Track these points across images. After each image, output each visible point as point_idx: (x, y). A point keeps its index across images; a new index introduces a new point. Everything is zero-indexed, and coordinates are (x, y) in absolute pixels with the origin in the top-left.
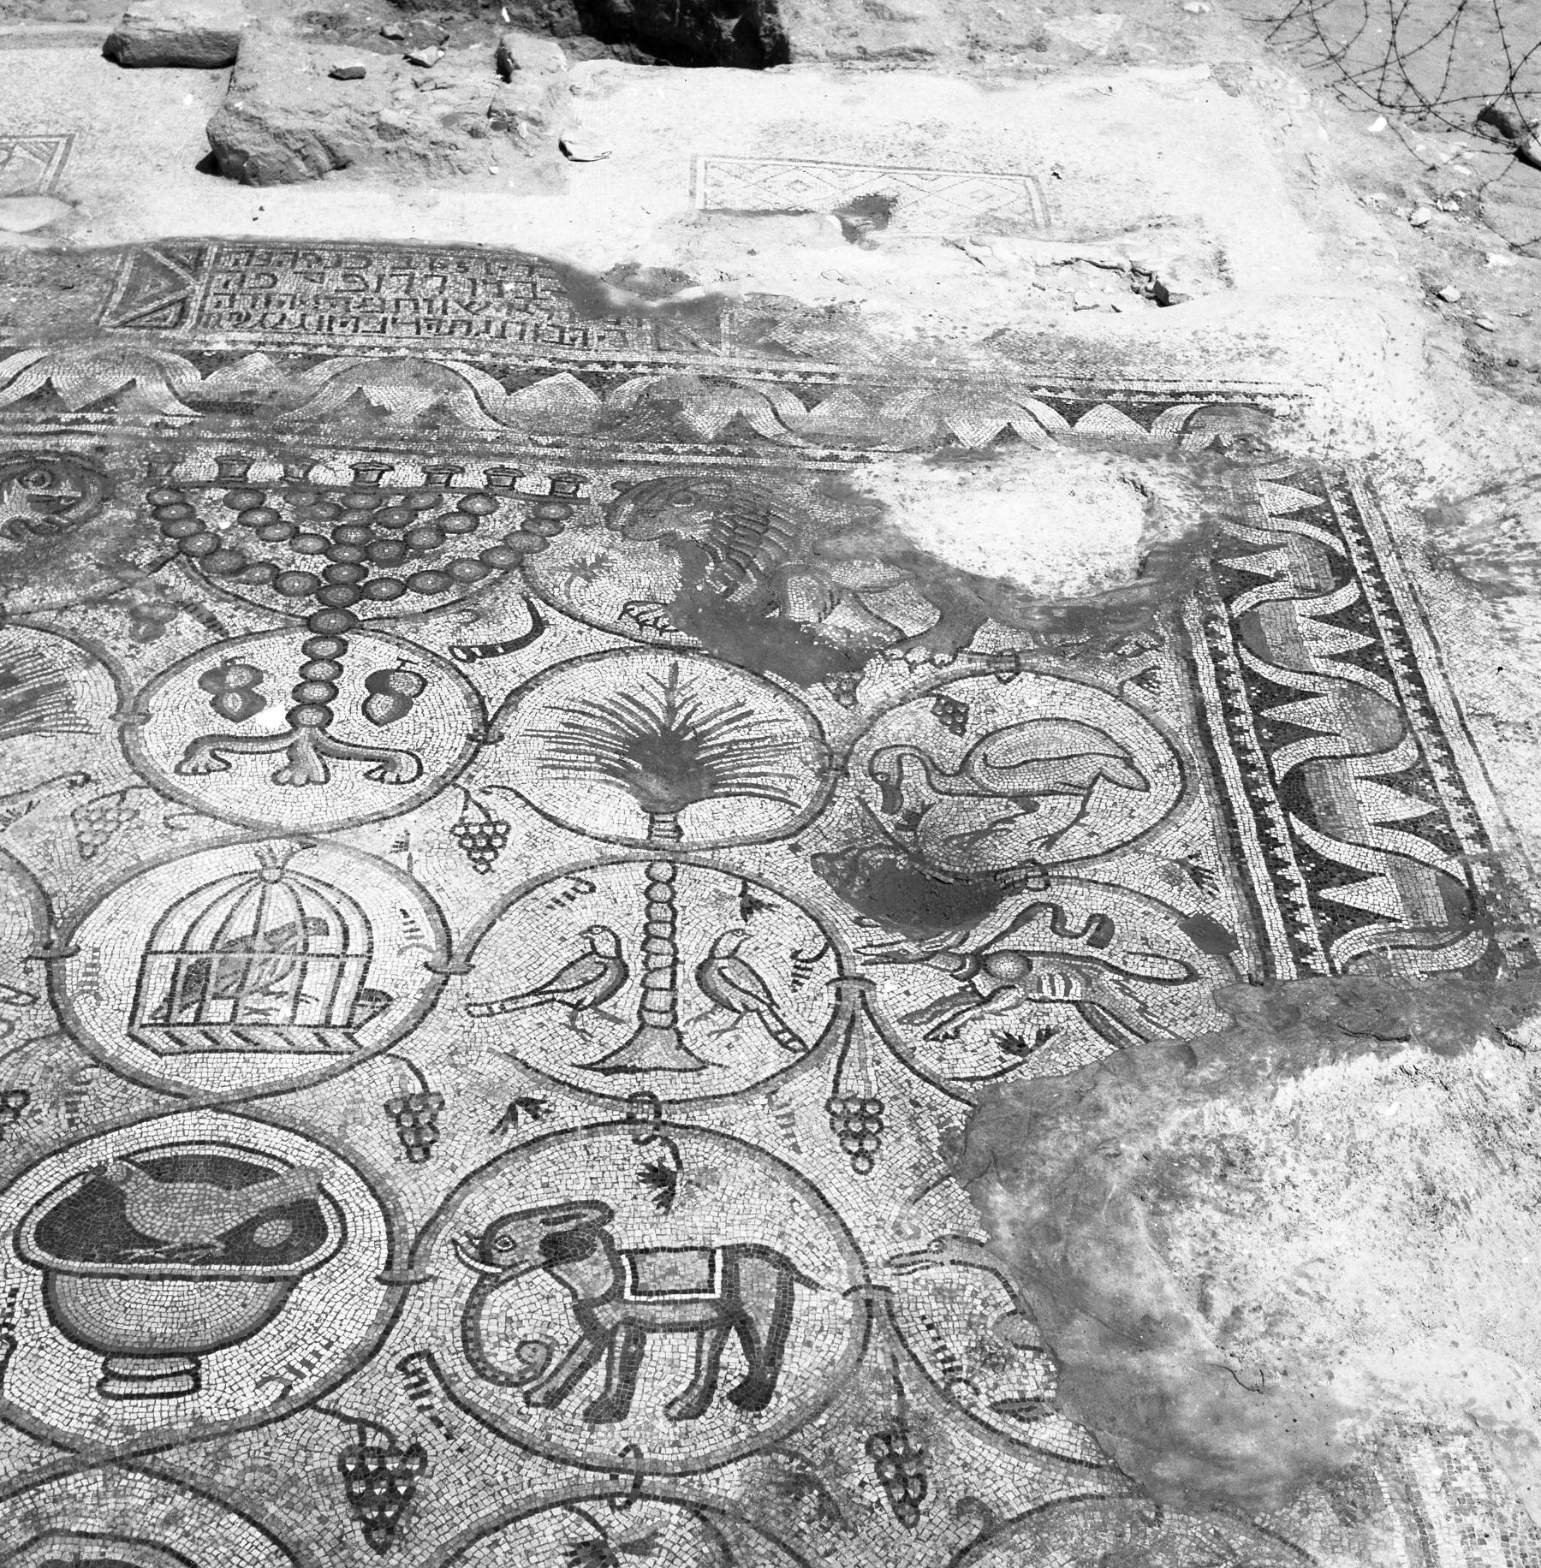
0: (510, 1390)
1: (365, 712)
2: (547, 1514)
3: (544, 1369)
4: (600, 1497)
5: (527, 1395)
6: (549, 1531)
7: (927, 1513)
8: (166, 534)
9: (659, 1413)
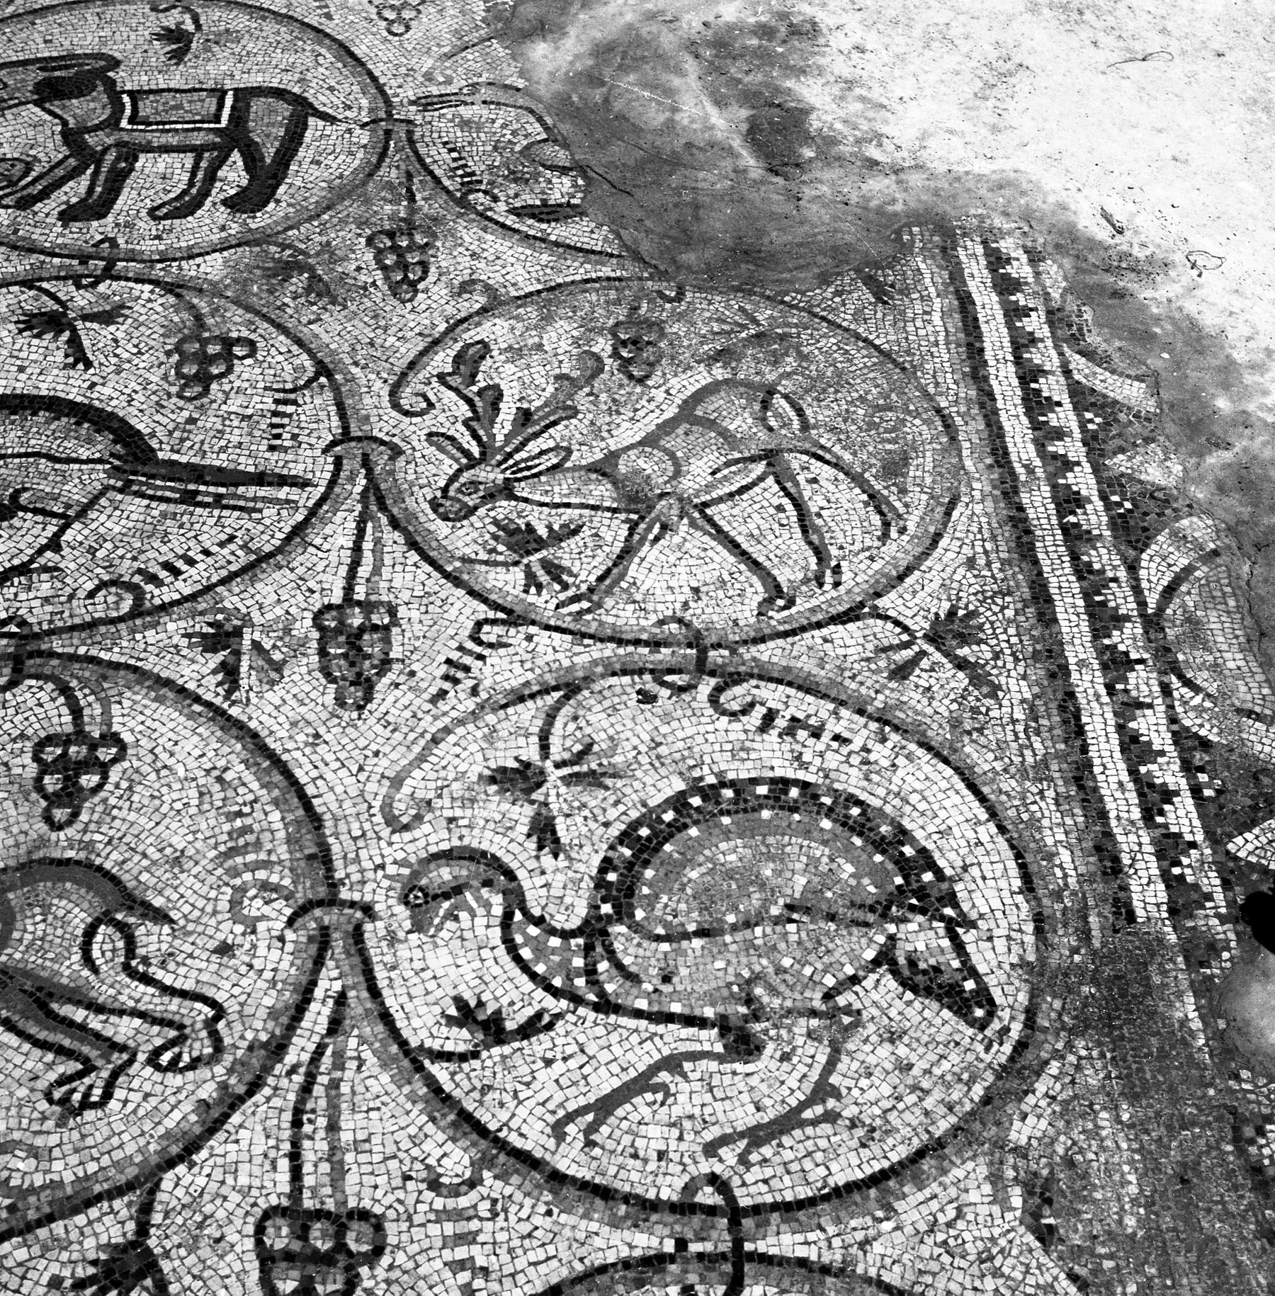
4: (65, 278)
7: (426, 291)
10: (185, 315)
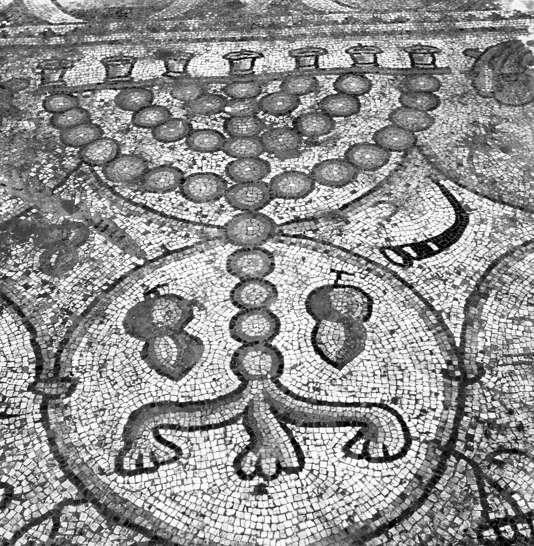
1: (318, 351)
8: (65, 144)
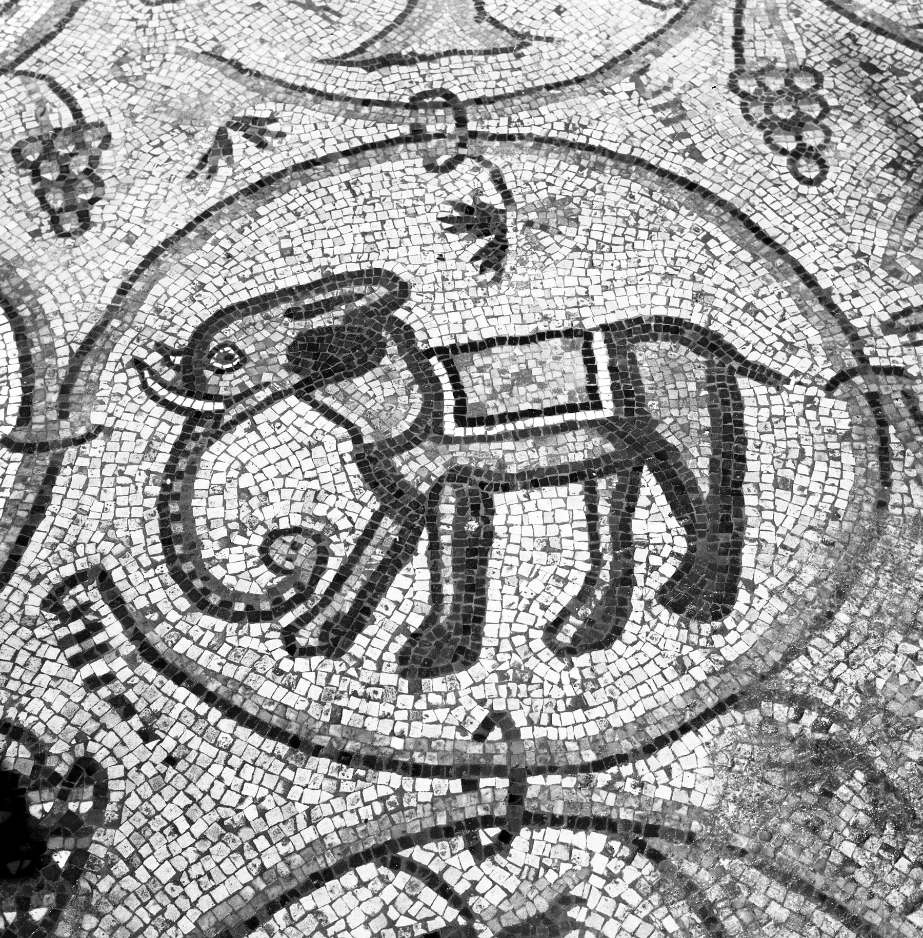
0: (257, 628)
2: (349, 880)
3: (315, 580)
4: (448, 832)
5: (289, 635)
6: (357, 919)
9: (538, 644)
10: (682, 910)
